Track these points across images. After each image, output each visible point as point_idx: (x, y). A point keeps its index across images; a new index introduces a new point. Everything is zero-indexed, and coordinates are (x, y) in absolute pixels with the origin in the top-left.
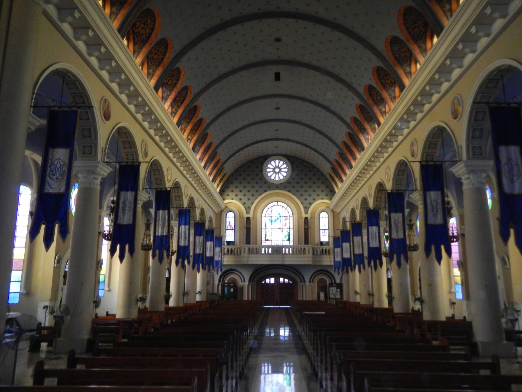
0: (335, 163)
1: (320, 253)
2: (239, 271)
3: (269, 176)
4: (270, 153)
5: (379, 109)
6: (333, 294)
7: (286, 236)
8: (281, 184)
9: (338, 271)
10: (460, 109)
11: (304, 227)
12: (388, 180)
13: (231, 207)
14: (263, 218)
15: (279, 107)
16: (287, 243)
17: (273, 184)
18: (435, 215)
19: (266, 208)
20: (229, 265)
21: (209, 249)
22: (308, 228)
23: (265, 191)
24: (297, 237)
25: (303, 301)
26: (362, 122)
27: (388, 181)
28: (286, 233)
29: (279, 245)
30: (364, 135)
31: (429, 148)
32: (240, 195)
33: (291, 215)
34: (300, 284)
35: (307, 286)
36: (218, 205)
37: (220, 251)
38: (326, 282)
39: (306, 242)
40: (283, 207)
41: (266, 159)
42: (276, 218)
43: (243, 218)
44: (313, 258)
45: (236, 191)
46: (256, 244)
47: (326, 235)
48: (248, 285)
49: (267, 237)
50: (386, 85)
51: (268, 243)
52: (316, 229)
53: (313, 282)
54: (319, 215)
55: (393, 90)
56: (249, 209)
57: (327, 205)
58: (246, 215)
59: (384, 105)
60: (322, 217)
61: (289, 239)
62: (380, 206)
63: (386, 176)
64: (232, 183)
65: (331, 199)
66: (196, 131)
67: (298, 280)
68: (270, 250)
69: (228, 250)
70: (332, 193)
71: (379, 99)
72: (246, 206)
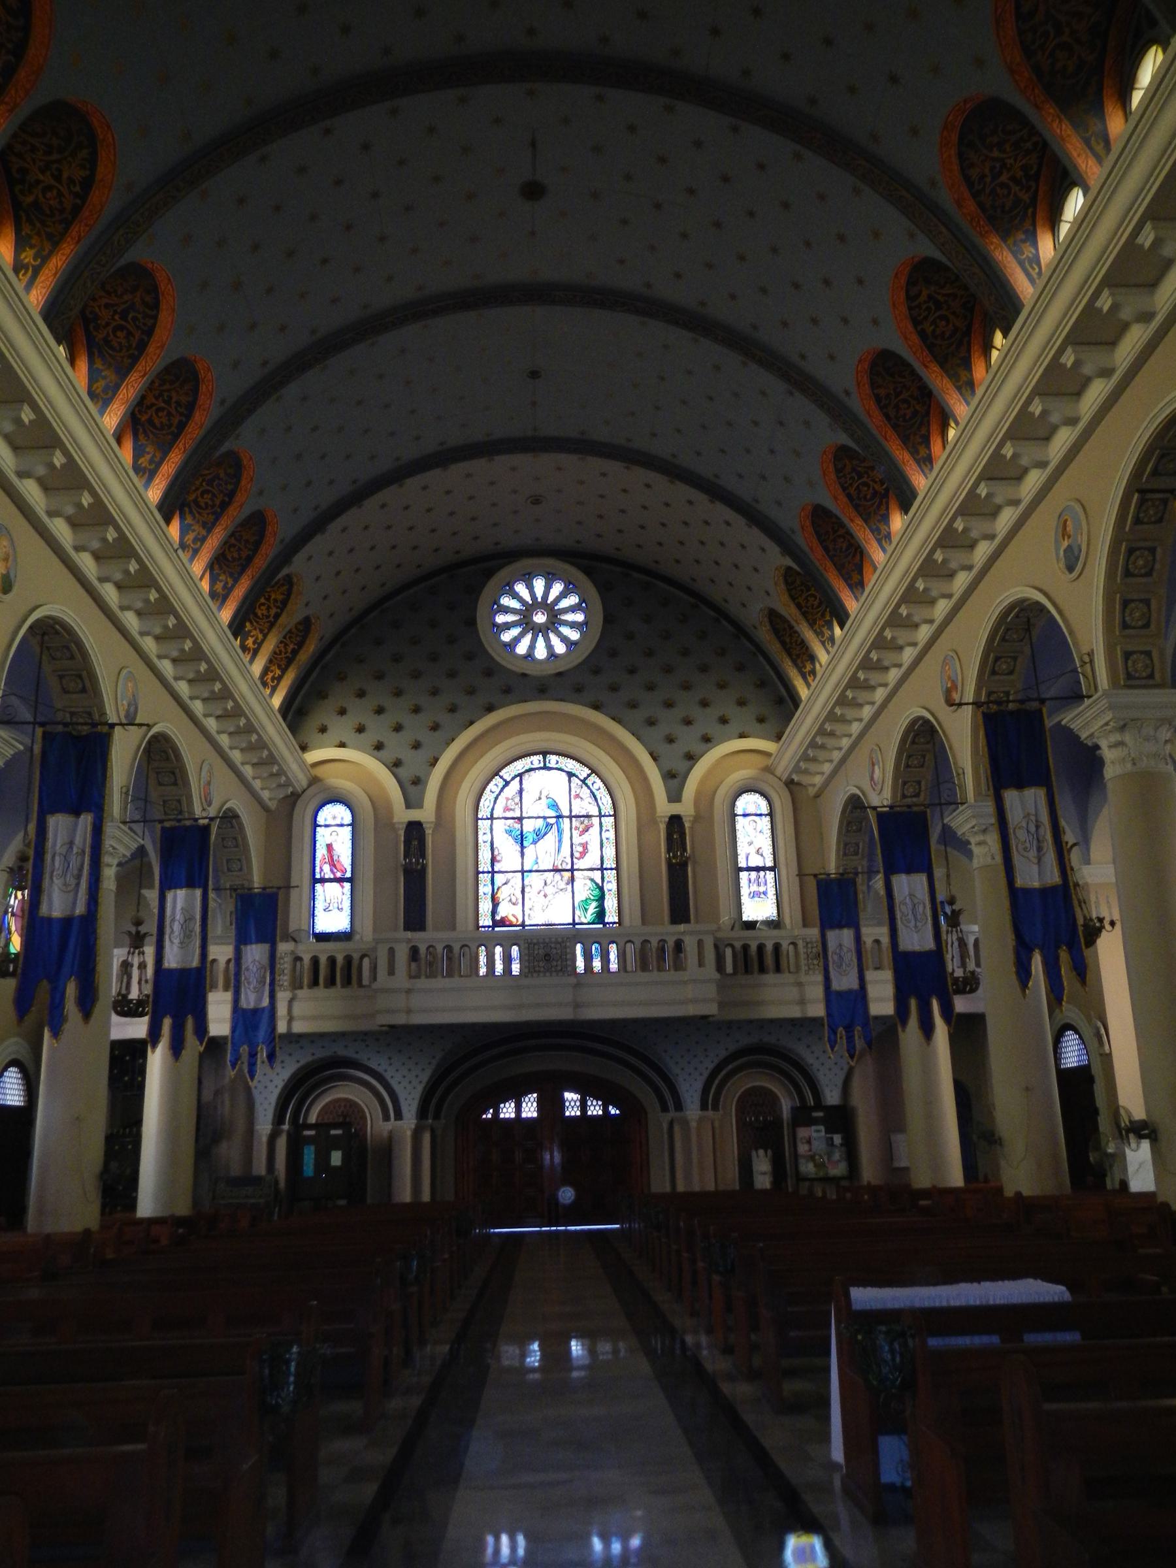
0: (805, 540)
2: (373, 1065)
3: (506, 645)
6: (812, 1158)
8: (560, 674)
9: (850, 1039)
13: (337, 780)
14: (483, 825)
17: (524, 675)
19: (495, 785)
20: (322, 1035)
21: (177, 927)
22: (684, 865)
23: (490, 709)
25: (674, 1195)
26: (917, 365)
28: (584, 888)
32: (378, 729)
33: (607, 807)
34: (658, 1120)
35: (693, 1124)
36: (268, 761)
37: (265, 961)
38: (774, 1100)
40: (570, 775)
41: (489, 574)
42: (540, 823)
43: (392, 826)
44: (721, 987)
45: (360, 712)
46: (453, 927)
48: (417, 1134)
53: (715, 1107)
54: (733, 805)
56: (419, 787)
58: (403, 815)
60: (745, 815)
61: (601, 914)
64: (342, 678)
65: (778, 737)
66: (68, 224)
68: (515, 951)
69: (315, 961)
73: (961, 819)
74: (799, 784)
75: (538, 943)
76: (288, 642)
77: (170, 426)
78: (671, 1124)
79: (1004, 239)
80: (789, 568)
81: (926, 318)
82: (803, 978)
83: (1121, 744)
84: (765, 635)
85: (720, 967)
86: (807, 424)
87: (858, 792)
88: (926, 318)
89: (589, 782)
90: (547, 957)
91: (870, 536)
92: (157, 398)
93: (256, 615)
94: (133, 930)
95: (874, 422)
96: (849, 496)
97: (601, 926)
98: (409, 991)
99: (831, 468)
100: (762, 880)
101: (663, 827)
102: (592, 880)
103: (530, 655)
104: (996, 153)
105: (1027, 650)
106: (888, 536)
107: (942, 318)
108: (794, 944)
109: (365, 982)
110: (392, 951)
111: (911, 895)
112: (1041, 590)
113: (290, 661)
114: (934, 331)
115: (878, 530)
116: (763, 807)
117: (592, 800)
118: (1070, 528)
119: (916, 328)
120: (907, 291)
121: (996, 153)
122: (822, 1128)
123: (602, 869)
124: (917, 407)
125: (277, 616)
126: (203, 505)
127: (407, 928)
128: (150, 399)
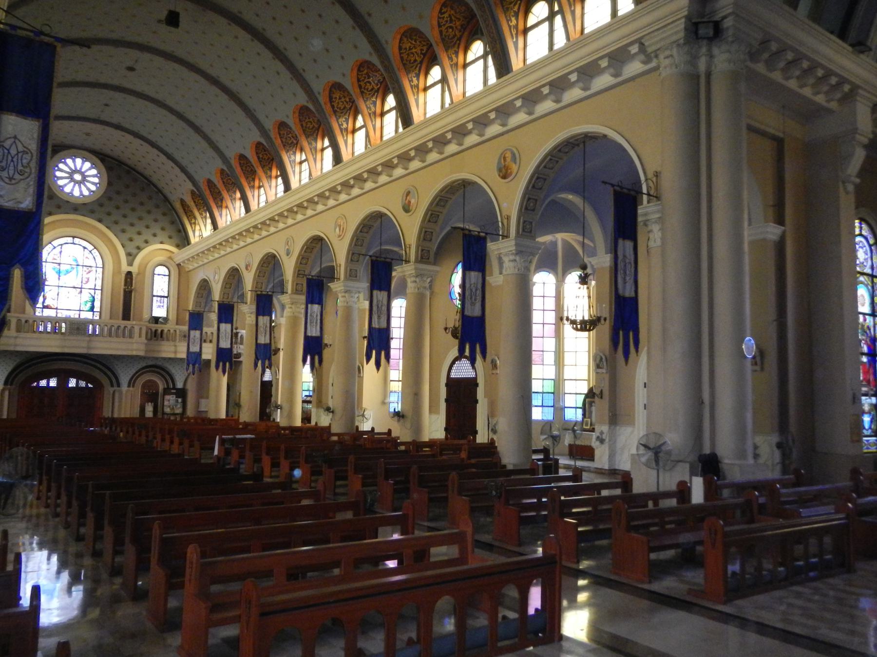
1: (151, 336)
5: (338, 122)
6: (169, 407)
7: (86, 302)
8: (84, 204)
10: (514, 168)
11: (125, 291)
12: (339, 236)
15: (135, 67)
16: (89, 315)
17: (68, 202)
18: (473, 304)
22: (131, 292)
24: (109, 306)
27: (342, 237)
28: (86, 296)
29: (72, 317)
30: (288, 154)
31: (437, 205)
33: (100, 264)
34: (109, 390)
35: (124, 392)
38: (157, 386)
39: (126, 316)
42: (69, 267)
47: (163, 306)
49: (46, 301)
50: (365, 91)
51: (47, 313)
53: (133, 386)
55: (373, 101)
57: (169, 254)
59: (346, 118)
60: (159, 275)
61: (92, 309)
62: (304, 271)
65: (178, 246)
67: (105, 381)
73: (245, 308)
75: (74, 323)
78: (114, 392)
79: (287, 152)
84: (178, 206)
87: (207, 278)
91: (229, 198)
98: (16, 338)
100: (162, 301)
101: (123, 275)
105: (273, 262)
108: (175, 331)
111: (225, 331)
116: (167, 273)
117: (94, 260)
118: (289, 243)
122: (175, 396)
123: (95, 289)
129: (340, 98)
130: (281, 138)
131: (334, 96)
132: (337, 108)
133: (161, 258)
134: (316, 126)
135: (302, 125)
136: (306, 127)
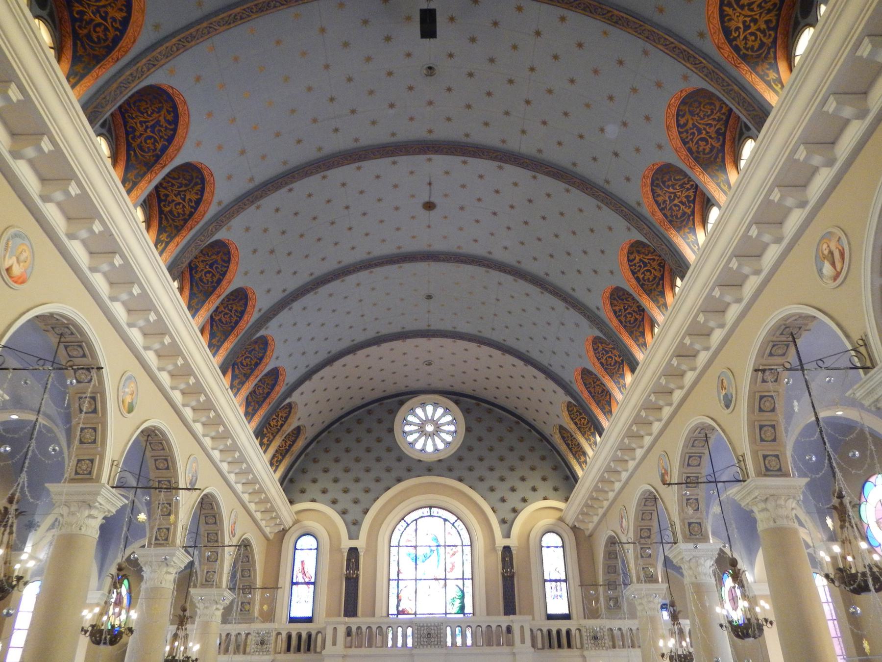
0: (579, 387)
3: (410, 444)
4: (414, 386)
8: (440, 461)
11: (503, 574)
12: (835, 279)
14: (394, 551)
15: (432, 200)
17: (420, 461)
22: (512, 577)
23: (399, 480)
26: (635, 295)
28: (453, 591)
30: (681, 233)
32: (335, 491)
33: (467, 541)
41: (402, 403)
43: (340, 550)
45: (325, 481)
46: (374, 615)
47: (560, 596)
49: (401, 603)
52: (535, 576)
57: (558, 514)
60: (548, 547)
61: (462, 608)
63: (820, 271)
65: (566, 500)
68: (410, 630)
69: (289, 637)
70: (570, 480)
71: (753, 47)
72: (350, 517)
74: (579, 528)
75: (423, 626)
76: (287, 440)
77: (231, 322)
79: (678, 231)
80: (570, 402)
81: (639, 271)
82: (586, 653)
83: (766, 510)
84: (557, 440)
85: (534, 645)
86: (577, 325)
88: (639, 271)
89: (456, 525)
90: (429, 635)
91: (614, 386)
92: (225, 308)
93: (270, 424)
94: (181, 613)
95: (613, 323)
96: (601, 363)
97: (462, 616)
98: (344, 656)
99: (591, 348)
100: (558, 588)
102: (457, 586)
103: (423, 450)
104: (671, 190)
105: (707, 452)
106: (624, 386)
107: (648, 270)
108: (579, 630)
109: (318, 650)
110: (335, 629)
112: (712, 419)
113: (287, 451)
114: (643, 278)
115: (619, 384)
119: (633, 275)
120: (628, 257)
121: (671, 190)
123: (463, 579)
124: (637, 317)
125: (282, 425)
126: (245, 364)
127: (346, 615)
128: (222, 308)
129: (746, 27)
130: (661, 210)
131: (733, 25)
132: (747, 49)
133: (548, 520)
134: (717, 145)
135: (690, 150)
136: (698, 152)
